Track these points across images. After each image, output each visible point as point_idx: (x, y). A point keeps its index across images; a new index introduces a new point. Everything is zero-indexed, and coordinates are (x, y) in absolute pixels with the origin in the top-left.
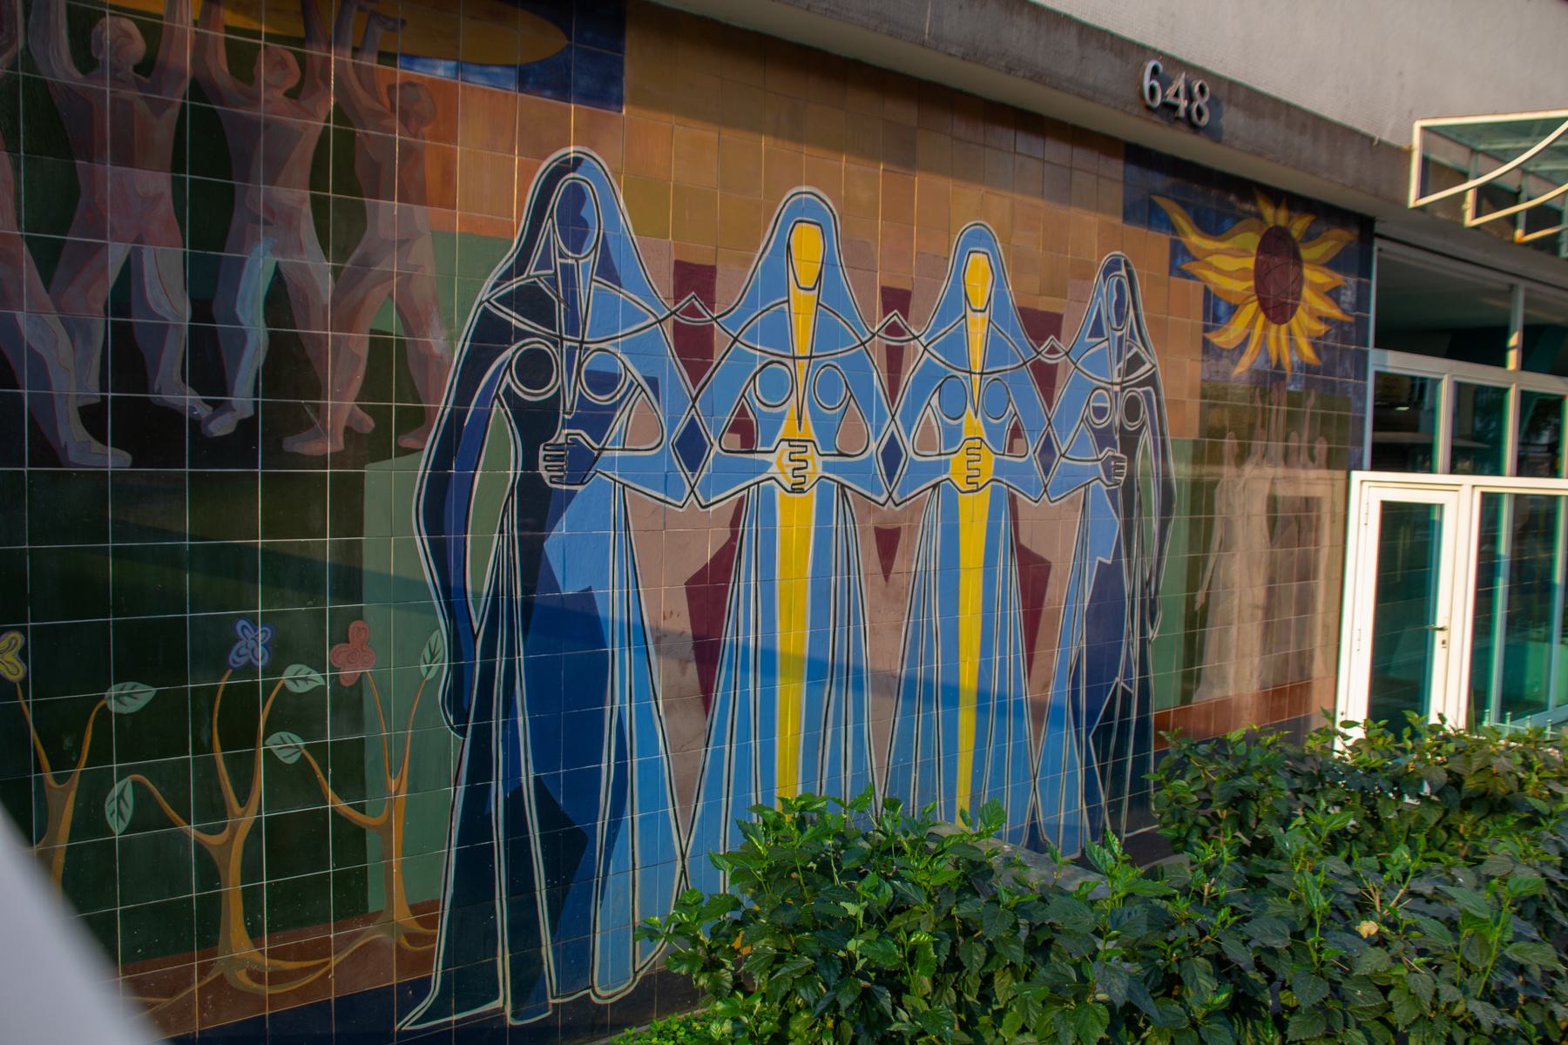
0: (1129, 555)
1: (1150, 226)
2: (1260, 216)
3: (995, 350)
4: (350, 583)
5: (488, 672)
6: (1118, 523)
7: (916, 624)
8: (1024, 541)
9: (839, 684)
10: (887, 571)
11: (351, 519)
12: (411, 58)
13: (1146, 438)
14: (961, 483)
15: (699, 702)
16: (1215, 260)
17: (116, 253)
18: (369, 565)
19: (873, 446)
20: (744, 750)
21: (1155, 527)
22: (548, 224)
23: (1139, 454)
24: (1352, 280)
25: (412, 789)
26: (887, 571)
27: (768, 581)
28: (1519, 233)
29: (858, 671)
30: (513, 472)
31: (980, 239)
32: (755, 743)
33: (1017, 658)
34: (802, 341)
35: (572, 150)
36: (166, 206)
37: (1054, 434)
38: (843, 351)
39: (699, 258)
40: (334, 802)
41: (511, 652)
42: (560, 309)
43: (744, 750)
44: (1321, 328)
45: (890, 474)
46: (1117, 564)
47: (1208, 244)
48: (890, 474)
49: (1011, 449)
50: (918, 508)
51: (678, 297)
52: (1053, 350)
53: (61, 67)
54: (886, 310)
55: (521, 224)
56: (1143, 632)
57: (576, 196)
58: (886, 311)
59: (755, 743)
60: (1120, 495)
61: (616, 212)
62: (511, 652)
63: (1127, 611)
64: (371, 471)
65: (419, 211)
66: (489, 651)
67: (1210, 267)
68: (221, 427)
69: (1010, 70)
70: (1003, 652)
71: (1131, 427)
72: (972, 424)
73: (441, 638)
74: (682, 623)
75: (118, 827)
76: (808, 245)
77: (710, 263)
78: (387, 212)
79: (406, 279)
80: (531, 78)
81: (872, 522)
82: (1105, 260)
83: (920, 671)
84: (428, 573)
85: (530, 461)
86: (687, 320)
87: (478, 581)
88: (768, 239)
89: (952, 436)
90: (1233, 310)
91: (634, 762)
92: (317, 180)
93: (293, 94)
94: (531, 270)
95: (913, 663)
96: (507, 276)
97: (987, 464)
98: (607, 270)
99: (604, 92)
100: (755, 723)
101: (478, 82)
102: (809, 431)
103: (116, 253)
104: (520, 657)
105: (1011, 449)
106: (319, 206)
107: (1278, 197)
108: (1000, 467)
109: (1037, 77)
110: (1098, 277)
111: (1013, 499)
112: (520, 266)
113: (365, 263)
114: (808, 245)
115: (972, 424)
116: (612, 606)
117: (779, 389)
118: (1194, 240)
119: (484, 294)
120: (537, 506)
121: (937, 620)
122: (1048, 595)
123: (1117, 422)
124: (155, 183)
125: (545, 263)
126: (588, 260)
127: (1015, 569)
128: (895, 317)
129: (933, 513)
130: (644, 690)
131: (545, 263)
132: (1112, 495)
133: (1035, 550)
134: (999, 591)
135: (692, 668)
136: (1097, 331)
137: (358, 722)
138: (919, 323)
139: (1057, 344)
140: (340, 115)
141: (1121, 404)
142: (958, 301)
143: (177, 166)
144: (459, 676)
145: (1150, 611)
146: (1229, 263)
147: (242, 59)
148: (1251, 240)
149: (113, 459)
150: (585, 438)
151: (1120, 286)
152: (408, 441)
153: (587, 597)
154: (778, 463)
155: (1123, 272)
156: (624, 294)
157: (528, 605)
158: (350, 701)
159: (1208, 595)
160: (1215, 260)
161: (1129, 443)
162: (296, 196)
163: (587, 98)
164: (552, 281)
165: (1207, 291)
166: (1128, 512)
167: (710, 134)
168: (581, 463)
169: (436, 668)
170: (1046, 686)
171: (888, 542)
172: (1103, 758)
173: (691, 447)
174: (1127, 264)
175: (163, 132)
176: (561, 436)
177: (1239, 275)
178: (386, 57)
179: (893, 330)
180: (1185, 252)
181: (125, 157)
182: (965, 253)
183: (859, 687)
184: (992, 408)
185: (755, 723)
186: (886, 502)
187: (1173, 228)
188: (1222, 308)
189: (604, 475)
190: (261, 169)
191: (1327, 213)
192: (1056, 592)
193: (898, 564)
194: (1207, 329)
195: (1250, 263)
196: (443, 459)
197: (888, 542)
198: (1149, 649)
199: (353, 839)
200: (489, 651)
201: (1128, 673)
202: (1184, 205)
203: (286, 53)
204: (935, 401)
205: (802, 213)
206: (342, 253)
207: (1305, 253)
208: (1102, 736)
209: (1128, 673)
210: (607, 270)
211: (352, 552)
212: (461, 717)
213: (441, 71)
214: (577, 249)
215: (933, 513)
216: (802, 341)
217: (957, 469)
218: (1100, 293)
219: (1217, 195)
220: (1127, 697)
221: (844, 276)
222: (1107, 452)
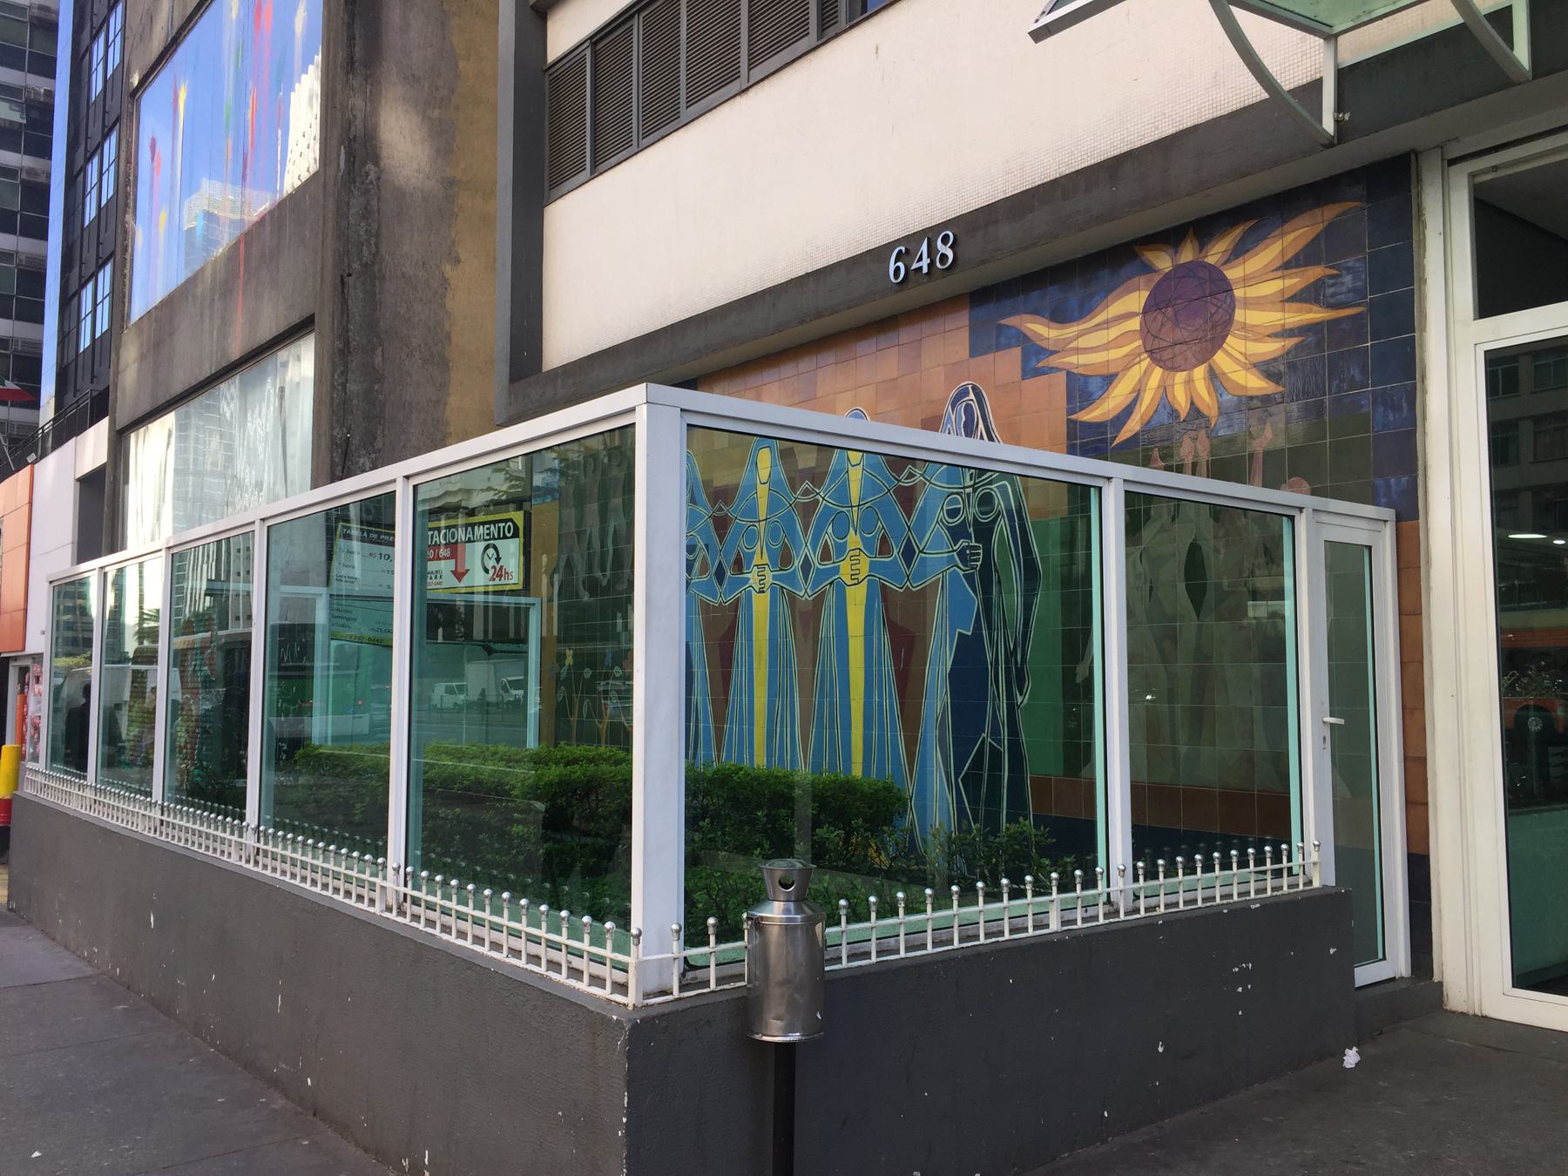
0: (989, 628)
3: (869, 486)
6: (977, 603)
13: (1002, 525)
16: (1083, 342)
20: (741, 730)
21: (1018, 600)
23: (995, 537)
27: (750, 640)
32: (746, 727)
34: (762, 514)
37: (914, 537)
38: (782, 512)
43: (741, 730)
44: (1291, 342)
47: (1071, 330)
52: (911, 476)
56: (1010, 696)
59: (746, 727)
63: (991, 675)
67: (1078, 351)
70: (880, 696)
71: (984, 520)
72: (853, 540)
82: (953, 393)
86: (718, 514)
89: (841, 550)
90: (1109, 380)
91: (701, 725)
100: (746, 716)
102: (766, 560)
108: (873, 566)
115: (853, 540)
117: (752, 538)
123: (971, 518)
127: (886, 640)
132: (970, 578)
141: (974, 500)
145: (1017, 679)
148: (1133, 300)
154: (753, 576)
155: (972, 396)
160: (1083, 342)
161: (984, 532)
166: (987, 591)
172: (974, 801)
173: (720, 575)
174: (974, 388)
184: (866, 526)
185: (746, 716)
188: (1094, 385)
194: (1071, 412)
195: (1135, 324)
198: (1019, 714)
201: (995, 733)
204: (830, 530)
207: (1233, 273)
208: (972, 781)
209: (995, 733)
216: (762, 514)
220: (996, 755)
222: (962, 543)
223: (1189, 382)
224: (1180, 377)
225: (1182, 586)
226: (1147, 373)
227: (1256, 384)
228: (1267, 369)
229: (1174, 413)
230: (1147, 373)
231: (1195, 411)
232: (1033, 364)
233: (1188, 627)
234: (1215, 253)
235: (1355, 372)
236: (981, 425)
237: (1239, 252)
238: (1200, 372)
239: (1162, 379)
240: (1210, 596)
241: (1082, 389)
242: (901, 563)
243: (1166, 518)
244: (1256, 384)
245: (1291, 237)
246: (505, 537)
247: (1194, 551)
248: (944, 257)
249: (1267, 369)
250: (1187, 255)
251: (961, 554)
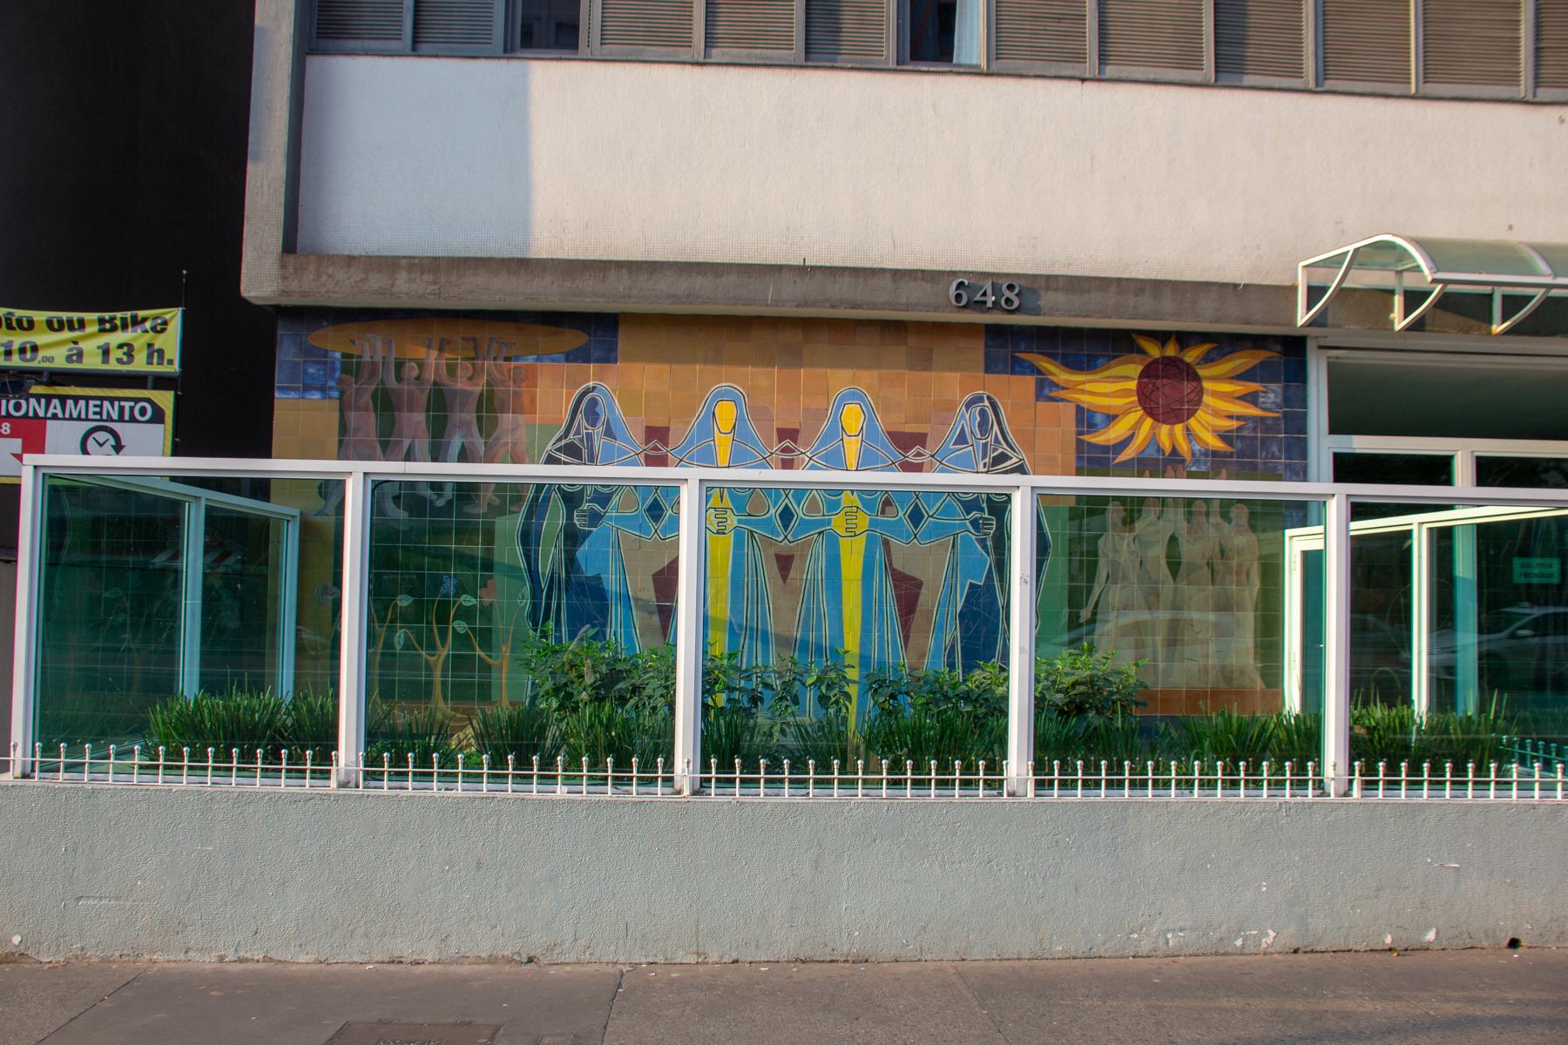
1: (1013, 372)
2: (1142, 351)
4: (488, 565)
5: (548, 606)
6: (989, 560)
7: (808, 609)
8: (897, 566)
9: (751, 638)
10: (784, 577)
11: (489, 537)
12: (517, 358)
14: (841, 532)
15: (660, 631)
16: (1087, 387)
17: (407, 443)
18: (496, 559)
19: (772, 511)
22: (579, 416)
24: (1277, 387)
25: (513, 651)
26: (784, 577)
28: (1497, 328)
29: (765, 633)
30: (562, 522)
31: (854, 396)
33: (894, 637)
35: (591, 384)
36: (424, 425)
39: (659, 422)
40: (478, 652)
41: (559, 599)
42: (585, 453)
44: (1235, 424)
45: (786, 527)
46: (989, 585)
48: (786, 527)
49: (883, 512)
50: (808, 544)
51: (647, 442)
52: (919, 454)
53: (392, 383)
54: (781, 439)
55: (567, 417)
57: (594, 402)
58: (781, 439)
60: (989, 543)
61: (614, 407)
62: (559, 599)
64: (498, 520)
65: (520, 417)
66: (549, 597)
67: (1083, 392)
68: (440, 503)
69: (833, 307)
70: (881, 630)
73: (527, 589)
74: (650, 595)
75: (398, 648)
76: (726, 413)
77: (665, 425)
78: (507, 419)
79: (515, 444)
80: (570, 357)
81: (772, 551)
82: (968, 397)
83: (812, 637)
84: (523, 564)
85: (570, 517)
86: (652, 453)
87: (544, 567)
88: (701, 411)
90: (1111, 418)
92: (479, 409)
93: (470, 379)
94: (571, 436)
95: (806, 629)
96: (560, 439)
97: (863, 521)
98: (609, 433)
99: (609, 357)
101: (548, 363)
102: (728, 502)
103: (407, 443)
104: (564, 601)
105: (883, 512)
106: (479, 419)
107: (1162, 337)
109: (856, 306)
110: (961, 408)
111: (886, 543)
112: (566, 434)
113: (497, 439)
114: (726, 413)
116: (612, 584)
118: (1062, 376)
119: (549, 447)
120: (573, 538)
121: (825, 607)
122: (922, 599)
124: (420, 417)
125: (578, 432)
126: (600, 429)
128: (787, 443)
129: (819, 548)
130: (628, 623)
131: (578, 432)
132: (982, 542)
133: (908, 572)
134: (876, 594)
135: (656, 618)
136: (961, 439)
137: (490, 620)
138: (806, 445)
139: (922, 450)
140: (488, 384)
142: (837, 431)
143: (428, 410)
144: (535, 608)
146: (1111, 389)
147: (452, 370)
148: (1134, 369)
149: (402, 514)
150: (597, 507)
151: (983, 413)
152: (514, 509)
153: (598, 578)
155: (986, 403)
156: (617, 444)
157: (568, 581)
158: (487, 612)
159: (1094, 614)
160: (1087, 387)
162: (471, 416)
163: (598, 361)
164: (581, 440)
165: (1080, 410)
167: (667, 367)
168: (595, 518)
169: (527, 603)
170: (922, 656)
171: (784, 563)
175: (424, 400)
176: (585, 506)
177: (1125, 393)
178: (507, 359)
179: (786, 450)
180: (1055, 385)
181: (411, 410)
182: (842, 403)
183: (765, 641)
186: (783, 540)
187: (1035, 370)
188: (1098, 419)
189: (605, 524)
190: (457, 407)
191: (1224, 344)
192: (928, 599)
193: (792, 574)
194: (1080, 433)
195: (1133, 385)
196: (529, 516)
197: (784, 563)
199: (486, 668)
200: (549, 597)
202: (1052, 357)
203: (468, 364)
205: (721, 397)
206: (488, 436)
210: (609, 433)
211: (489, 552)
212: (535, 624)
213: (531, 359)
214: (593, 425)
215: (819, 548)
217: (838, 523)
218: (963, 417)
219: (1089, 347)
221: (751, 427)
222: (975, 514)
223: (1172, 435)
224: (1165, 428)
225: (1163, 562)
226: (1139, 423)
227: (1215, 443)
228: (1225, 437)
229: (1160, 450)
230: (1139, 423)
231: (1174, 451)
232: (1046, 391)
233: (1167, 588)
234: (1191, 356)
235: (1275, 449)
236: (996, 427)
237: (1207, 360)
238: (1179, 429)
239: (1153, 428)
240: (1183, 570)
241: (1086, 419)
242: (909, 525)
243: (1152, 517)
244: (1215, 443)
245: (1238, 362)
246: (133, 420)
247: (1173, 540)
248: (1008, 301)
249: (1225, 437)
250: (1171, 350)
251: (974, 523)
